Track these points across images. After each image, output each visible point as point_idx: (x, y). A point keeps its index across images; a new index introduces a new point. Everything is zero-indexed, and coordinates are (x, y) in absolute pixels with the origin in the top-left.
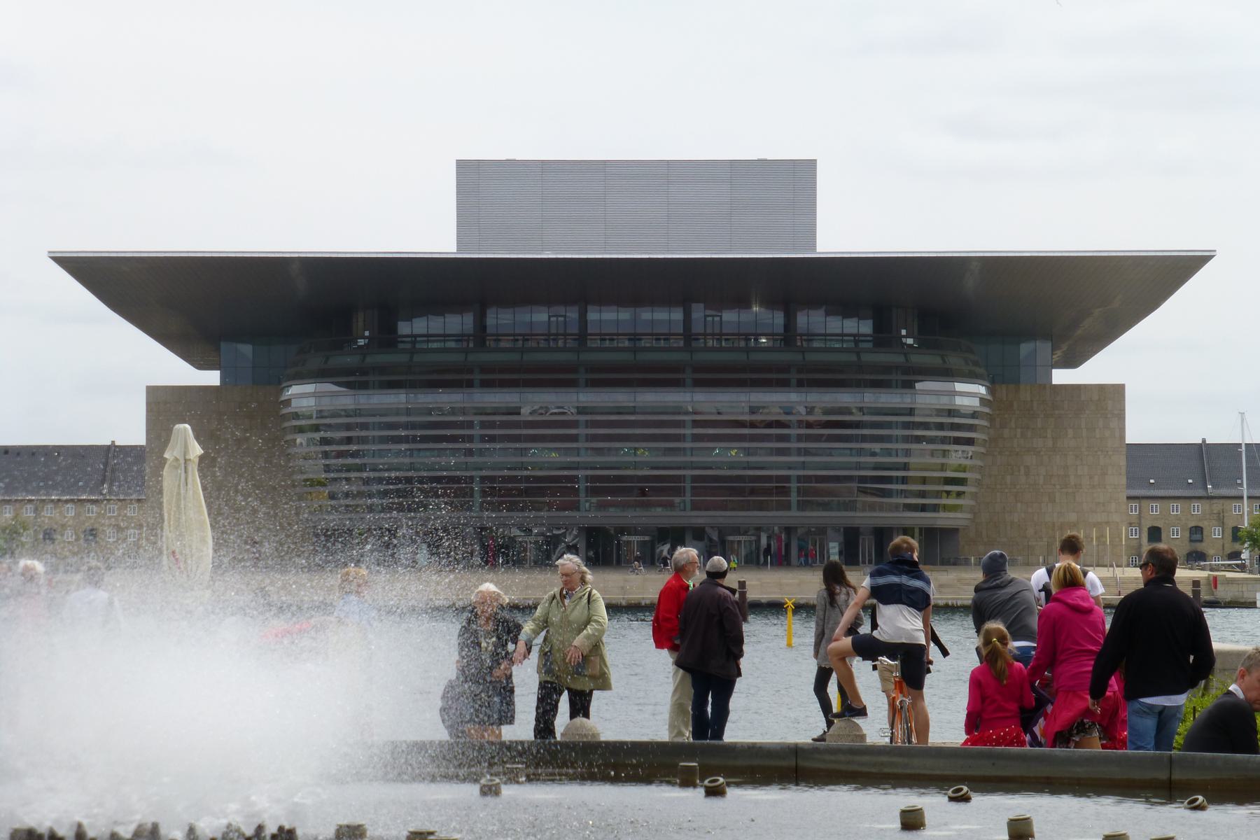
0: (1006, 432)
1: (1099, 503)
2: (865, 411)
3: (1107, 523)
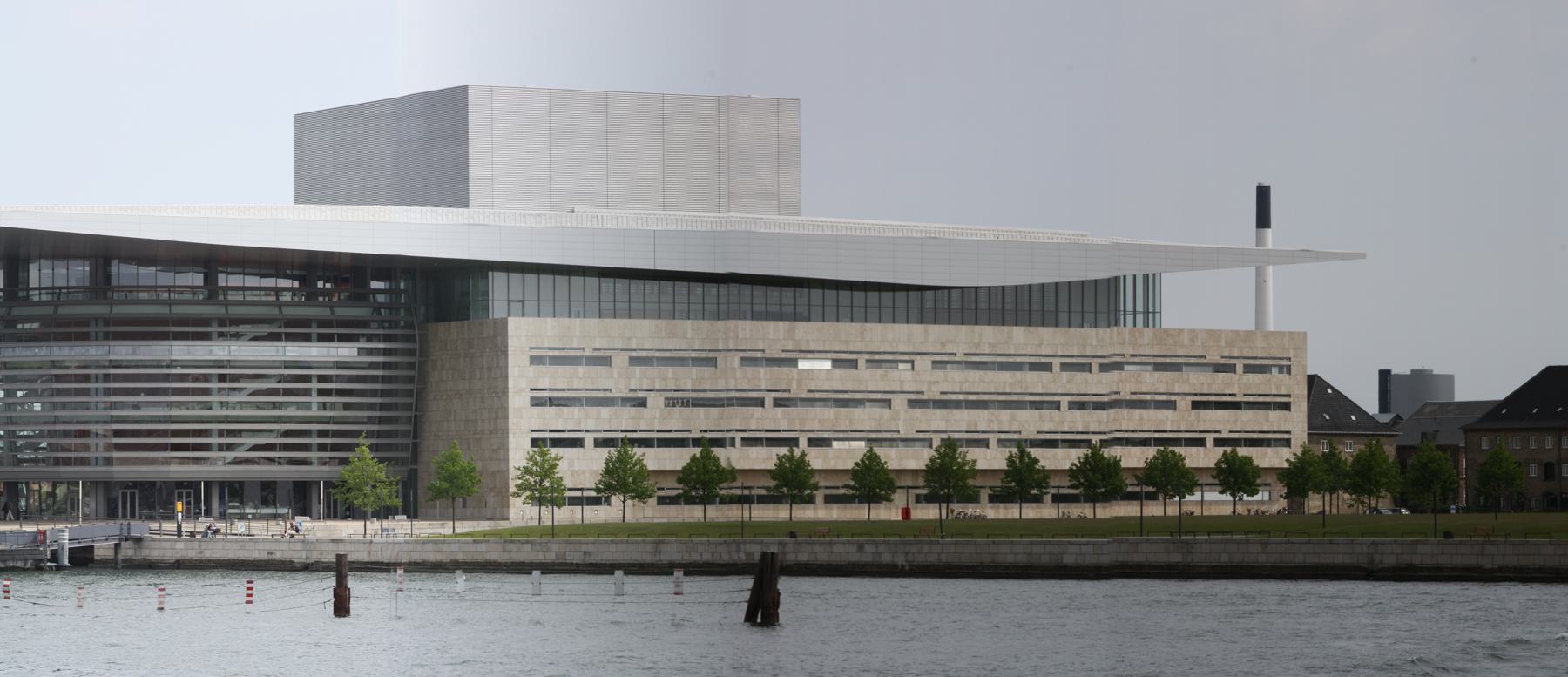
0: (444, 372)
1: (493, 450)
2: (8, 366)
3: (498, 471)
